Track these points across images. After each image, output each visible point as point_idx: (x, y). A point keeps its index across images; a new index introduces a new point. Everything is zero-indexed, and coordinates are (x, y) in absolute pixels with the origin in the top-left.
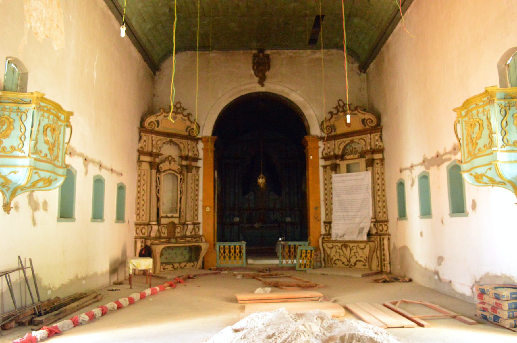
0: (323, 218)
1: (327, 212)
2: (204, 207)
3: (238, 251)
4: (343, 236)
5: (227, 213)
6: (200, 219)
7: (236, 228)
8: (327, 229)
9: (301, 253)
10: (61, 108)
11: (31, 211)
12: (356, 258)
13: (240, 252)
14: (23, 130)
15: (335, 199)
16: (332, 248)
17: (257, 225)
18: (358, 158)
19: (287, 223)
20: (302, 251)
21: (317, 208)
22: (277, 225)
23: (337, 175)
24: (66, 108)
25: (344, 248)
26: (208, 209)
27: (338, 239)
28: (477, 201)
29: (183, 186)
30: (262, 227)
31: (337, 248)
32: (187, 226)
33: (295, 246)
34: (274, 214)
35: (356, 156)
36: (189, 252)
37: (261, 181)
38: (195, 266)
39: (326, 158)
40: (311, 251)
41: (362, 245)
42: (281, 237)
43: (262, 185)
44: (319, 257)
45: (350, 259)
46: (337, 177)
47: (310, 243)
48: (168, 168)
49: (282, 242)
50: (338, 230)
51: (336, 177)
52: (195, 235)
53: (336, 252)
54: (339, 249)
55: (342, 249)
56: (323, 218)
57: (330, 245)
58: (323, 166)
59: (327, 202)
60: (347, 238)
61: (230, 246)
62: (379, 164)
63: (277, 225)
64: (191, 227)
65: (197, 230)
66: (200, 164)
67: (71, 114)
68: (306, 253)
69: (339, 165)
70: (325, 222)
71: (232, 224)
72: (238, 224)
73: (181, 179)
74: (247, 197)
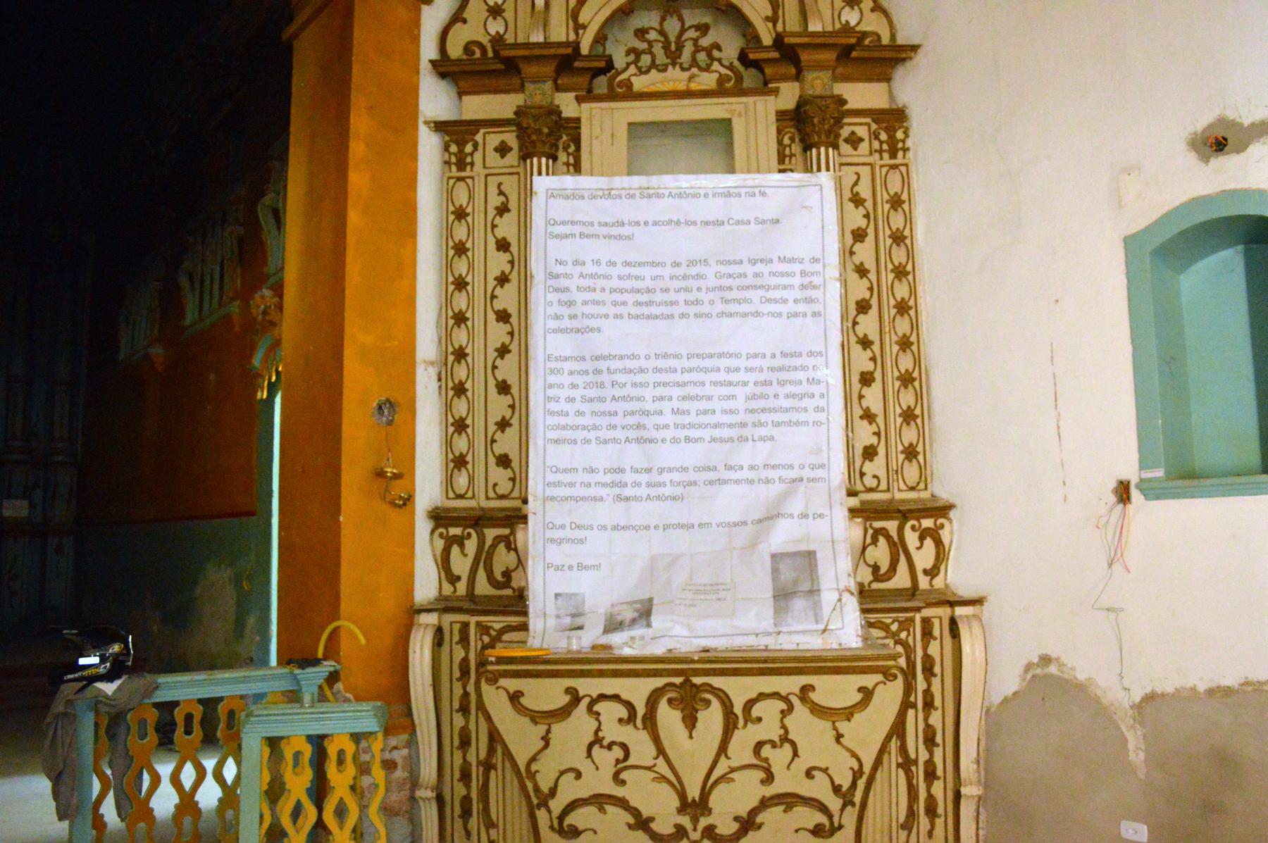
0: (428, 488)
1: (461, 444)
4: (645, 613)
8: (461, 565)
12: (769, 778)
16: (563, 713)
18: (721, 91)
21: (394, 411)
23: (569, 181)
25: (669, 717)
27: (626, 644)
33: (209, 704)
35: (708, 80)
41: (836, 690)
42: (97, 641)
44: (400, 774)
45: (705, 794)
46: (576, 195)
47: (333, 678)
49: (109, 688)
50: (576, 574)
53: (597, 740)
54: (632, 718)
58: (440, 127)
59: (461, 372)
60: (676, 633)
62: (864, 147)
69: (572, 128)
70: (440, 518)
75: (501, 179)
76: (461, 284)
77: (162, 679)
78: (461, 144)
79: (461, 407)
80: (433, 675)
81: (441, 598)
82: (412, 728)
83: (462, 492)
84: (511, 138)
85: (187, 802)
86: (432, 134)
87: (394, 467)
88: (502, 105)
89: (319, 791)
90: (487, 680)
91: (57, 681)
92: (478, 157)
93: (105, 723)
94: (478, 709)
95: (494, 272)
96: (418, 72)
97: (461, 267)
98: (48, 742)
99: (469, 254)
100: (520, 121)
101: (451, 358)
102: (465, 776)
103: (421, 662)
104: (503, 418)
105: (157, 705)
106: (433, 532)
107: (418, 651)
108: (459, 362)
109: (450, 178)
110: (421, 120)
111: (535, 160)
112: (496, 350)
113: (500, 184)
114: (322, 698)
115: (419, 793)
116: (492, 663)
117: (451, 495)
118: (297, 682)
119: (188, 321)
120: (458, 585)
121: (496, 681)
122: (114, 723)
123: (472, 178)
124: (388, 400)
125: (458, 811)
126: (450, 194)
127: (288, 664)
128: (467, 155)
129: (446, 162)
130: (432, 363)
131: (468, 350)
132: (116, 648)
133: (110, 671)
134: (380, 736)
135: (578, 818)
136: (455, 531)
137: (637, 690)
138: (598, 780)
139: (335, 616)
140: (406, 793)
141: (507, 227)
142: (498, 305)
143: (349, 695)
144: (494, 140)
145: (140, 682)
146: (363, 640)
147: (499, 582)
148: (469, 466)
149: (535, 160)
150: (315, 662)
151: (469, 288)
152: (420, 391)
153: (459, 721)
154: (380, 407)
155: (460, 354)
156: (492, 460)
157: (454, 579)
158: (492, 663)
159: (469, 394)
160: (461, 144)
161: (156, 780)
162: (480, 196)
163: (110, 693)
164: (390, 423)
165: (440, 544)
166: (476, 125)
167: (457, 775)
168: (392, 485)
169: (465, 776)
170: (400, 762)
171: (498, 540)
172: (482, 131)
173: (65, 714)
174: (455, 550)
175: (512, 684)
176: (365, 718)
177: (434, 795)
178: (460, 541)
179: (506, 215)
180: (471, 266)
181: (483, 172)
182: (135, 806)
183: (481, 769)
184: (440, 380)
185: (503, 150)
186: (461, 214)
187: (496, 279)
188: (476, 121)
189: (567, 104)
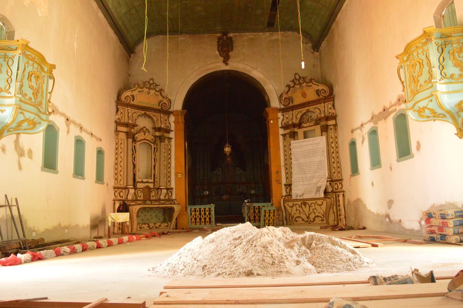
0: (284, 181)
1: (287, 176)
2: (176, 174)
3: (207, 213)
4: (302, 195)
6: (173, 185)
8: (288, 191)
9: (265, 212)
10: (45, 59)
11: (17, 156)
12: (315, 214)
13: (210, 214)
14: (9, 74)
15: (294, 162)
16: (293, 206)
17: (224, 197)
18: (314, 125)
20: (265, 211)
21: (278, 172)
23: (295, 141)
24: (50, 60)
25: (303, 206)
28: (420, 142)
29: (157, 154)
30: (229, 198)
31: (297, 206)
32: (161, 191)
33: (259, 207)
34: (240, 187)
35: (312, 124)
37: (227, 149)
38: (169, 227)
39: (285, 127)
40: (274, 211)
41: (319, 202)
43: (228, 154)
44: (281, 216)
45: (309, 215)
46: (296, 143)
48: (143, 138)
49: (248, 204)
50: (297, 191)
51: (294, 143)
53: (297, 210)
54: (299, 207)
55: (301, 206)
56: (284, 181)
57: (291, 204)
58: (282, 135)
59: (287, 166)
60: (305, 197)
61: (200, 209)
62: (333, 130)
64: (164, 191)
65: (170, 195)
66: (172, 135)
67: (53, 67)
68: (270, 213)
69: (297, 133)
70: (285, 185)
73: (155, 148)
76: (286, 155)
79: (287, 171)
82: (282, 211)
135: (297, 219)
137: (299, 203)
138: (298, 215)
150: (270, 202)
168: (279, 182)
175: (287, 203)
189: (296, 130)
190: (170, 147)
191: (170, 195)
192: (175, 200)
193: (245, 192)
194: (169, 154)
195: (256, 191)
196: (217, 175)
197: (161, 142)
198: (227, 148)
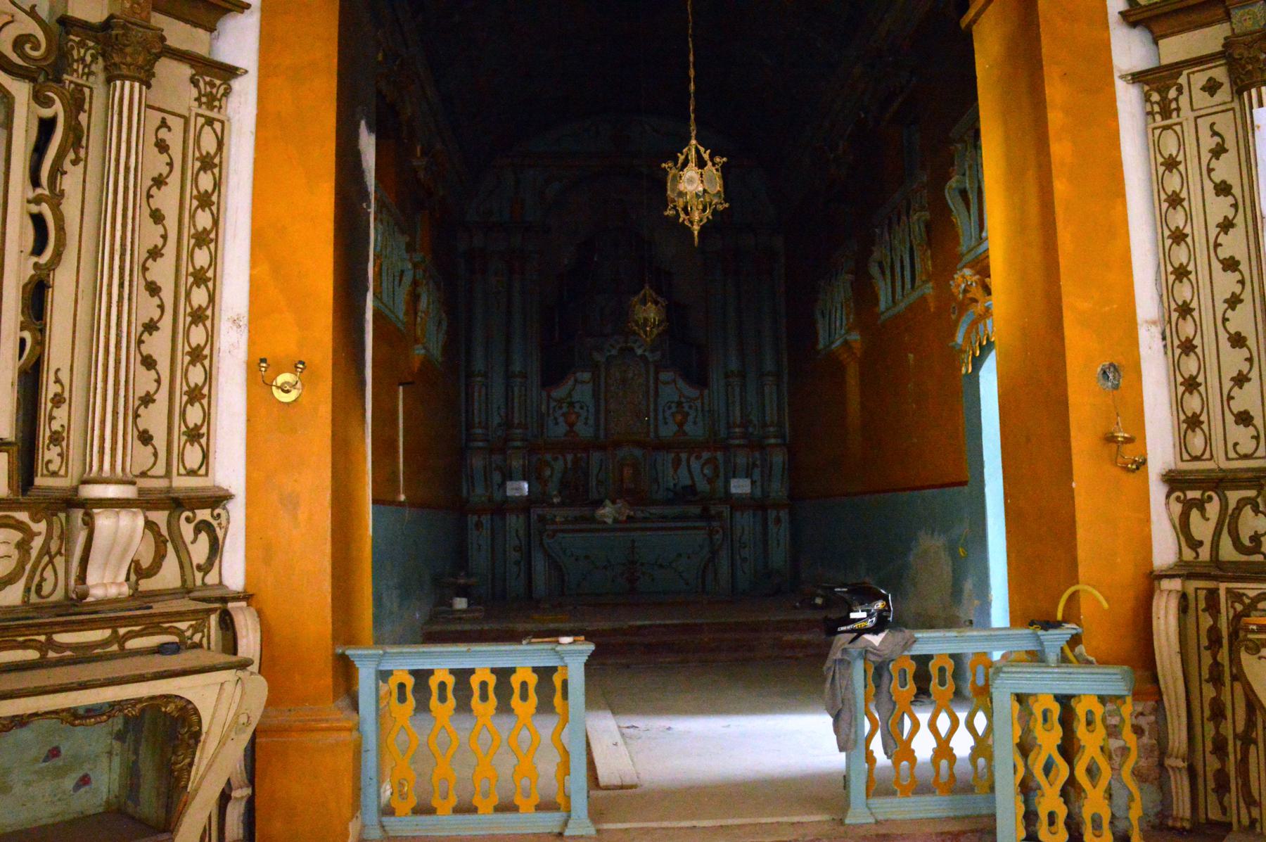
0: (1160, 450)
1: (1193, 404)
2: (260, 371)
5: (477, 462)
6: (229, 468)
7: (515, 522)
8: (1202, 528)
17: (607, 512)
19: (738, 504)
21: (1120, 374)
22: (695, 510)
26: (286, 388)
29: (70, 182)
30: (630, 519)
32: (89, 524)
34: (677, 463)
36: (120, 737)
37: (695, 184)
47: (1075, 641)
49: (876, 640)
52: (185, 590)
56: (1160, 450)
58: (1137, 78)
59: (1187, 329)
63: (695, 510)
68: (1067, 720)
70: (1174, 481)
71: (502, 508)
72: (524, 506)
73: (46, 127)
74: (560, 392)
75: (1210, 119)
77: (918, 635)
78: (1163, 91)
79: (1190, 366)
80: (1180, 642)
81: (1181, 563)
83: (1199, 454)
84: (1220, 73)
85: (943, 749)
86: (1130, 86)
87: (1125, 431)
88: (1209, 39)
89: (1068, 749)
90: (1247, 649)
91: (833, 632)
92: (1184, 100)
93: (871, 671)
94: (1234, 678)
95: (1215, 218)
96: (1107, 27)
97: (1177, 219)
98: (828, 685)
99: (1185, 204)
100: (1227, 54)
101: (1175, 315)
102: (1220, 748)
103: (1167, 629)
104: (1240, 372)
105: (913, 657)
106: (1168, 496)
107: (1162, 621)
108: (1184, 319)
109: (1154, 129)
110: (1116, 75)
111: (1254, 91)
112: (1226, 301)
113: (1212, 125)
114: (1064, 660)
115: (1169, 762)
116: (1253, 631)
117: (1186, 457)
118: (1041, 644)
119: (882, 306)
120: (1200, 550)
121: (1259, 651)
122: (879, 672)
123: (1180, 124)
124: (1111, 365)
125: (1211, 784)
126: (1157, 146)
127: (1032, 624)
128: (1171, 101)
129: (1148, 113)
130: (1154, 323)
131: (1194, 305)
132: (880, 605)
133: (876, 625)
134: (1129, 700)
136: (1193, 494)
139: (1074, 580)
140: (1154, 760)
141: (1226, 169)
142: (1224, 253)
143: (1091, 658)
144: (1200, 79)
145: (899, 637)
146: (1106, 605)
147: (1248, 548)
148: (1205, 426)
149: (1254, 91)
150: (1057, 625)
151: (1189, 240)
152: (1144, 351)
153: (1209, 692)
154: (1105, 372)
155: (1185, 310)
156: (1230, 419)
157: (1195, 545)
158: (1253, 631)
159: (1198, 350)
160: (1163, 91)
161: (916, 726)
162: (1191, 141)
163: (877, 644)
164: (1116, 387)
165: (1177, 508)
166: (1176, 68)
167: (1209, 746)
168: (1123, 448)
169: (1220, 748)
170: (1146, 727)
171: (1242, 503)
172: (1185, 73)
173: (841, 661)
174: (1195, 514)
176: (1115, 681)
177: (1186, 764)
178: (1200, 505)
179: (1223, 156)
180: (1189, 217)
181: (1192, 115)
182: (899, 748)
183: (1239, 743)
184: (1164, 338)
185: (1211, 87)
186: (1171, 164)
187: (1218, 226)
188: (1177, 63)
190: (209, 144)
191: (200, 550)
192: (246, 597)
193: (702, 486)
194: (205, 201)
195: (753, 483)
196: (571, 404)
197: (109, 80)
198: (691, 172)
